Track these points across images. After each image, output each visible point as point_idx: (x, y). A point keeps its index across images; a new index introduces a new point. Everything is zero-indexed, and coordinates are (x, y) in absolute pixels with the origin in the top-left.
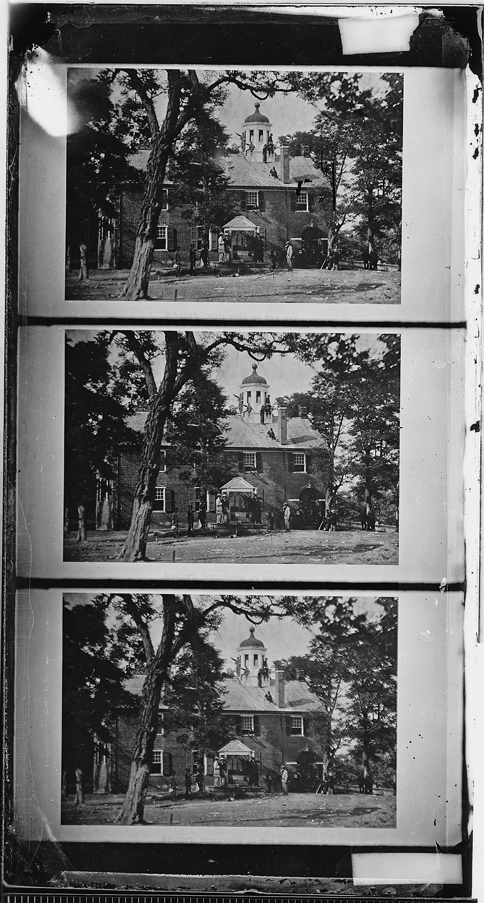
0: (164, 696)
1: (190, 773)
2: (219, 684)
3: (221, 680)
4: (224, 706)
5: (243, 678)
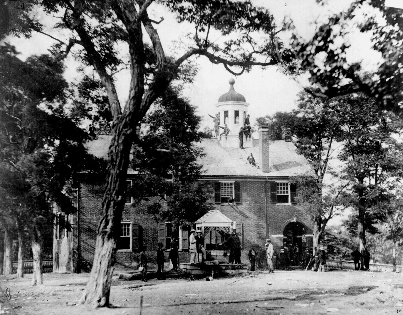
1: (163, 248)
2: (196, 145)
4: (201, 170)
5: (222, 138)
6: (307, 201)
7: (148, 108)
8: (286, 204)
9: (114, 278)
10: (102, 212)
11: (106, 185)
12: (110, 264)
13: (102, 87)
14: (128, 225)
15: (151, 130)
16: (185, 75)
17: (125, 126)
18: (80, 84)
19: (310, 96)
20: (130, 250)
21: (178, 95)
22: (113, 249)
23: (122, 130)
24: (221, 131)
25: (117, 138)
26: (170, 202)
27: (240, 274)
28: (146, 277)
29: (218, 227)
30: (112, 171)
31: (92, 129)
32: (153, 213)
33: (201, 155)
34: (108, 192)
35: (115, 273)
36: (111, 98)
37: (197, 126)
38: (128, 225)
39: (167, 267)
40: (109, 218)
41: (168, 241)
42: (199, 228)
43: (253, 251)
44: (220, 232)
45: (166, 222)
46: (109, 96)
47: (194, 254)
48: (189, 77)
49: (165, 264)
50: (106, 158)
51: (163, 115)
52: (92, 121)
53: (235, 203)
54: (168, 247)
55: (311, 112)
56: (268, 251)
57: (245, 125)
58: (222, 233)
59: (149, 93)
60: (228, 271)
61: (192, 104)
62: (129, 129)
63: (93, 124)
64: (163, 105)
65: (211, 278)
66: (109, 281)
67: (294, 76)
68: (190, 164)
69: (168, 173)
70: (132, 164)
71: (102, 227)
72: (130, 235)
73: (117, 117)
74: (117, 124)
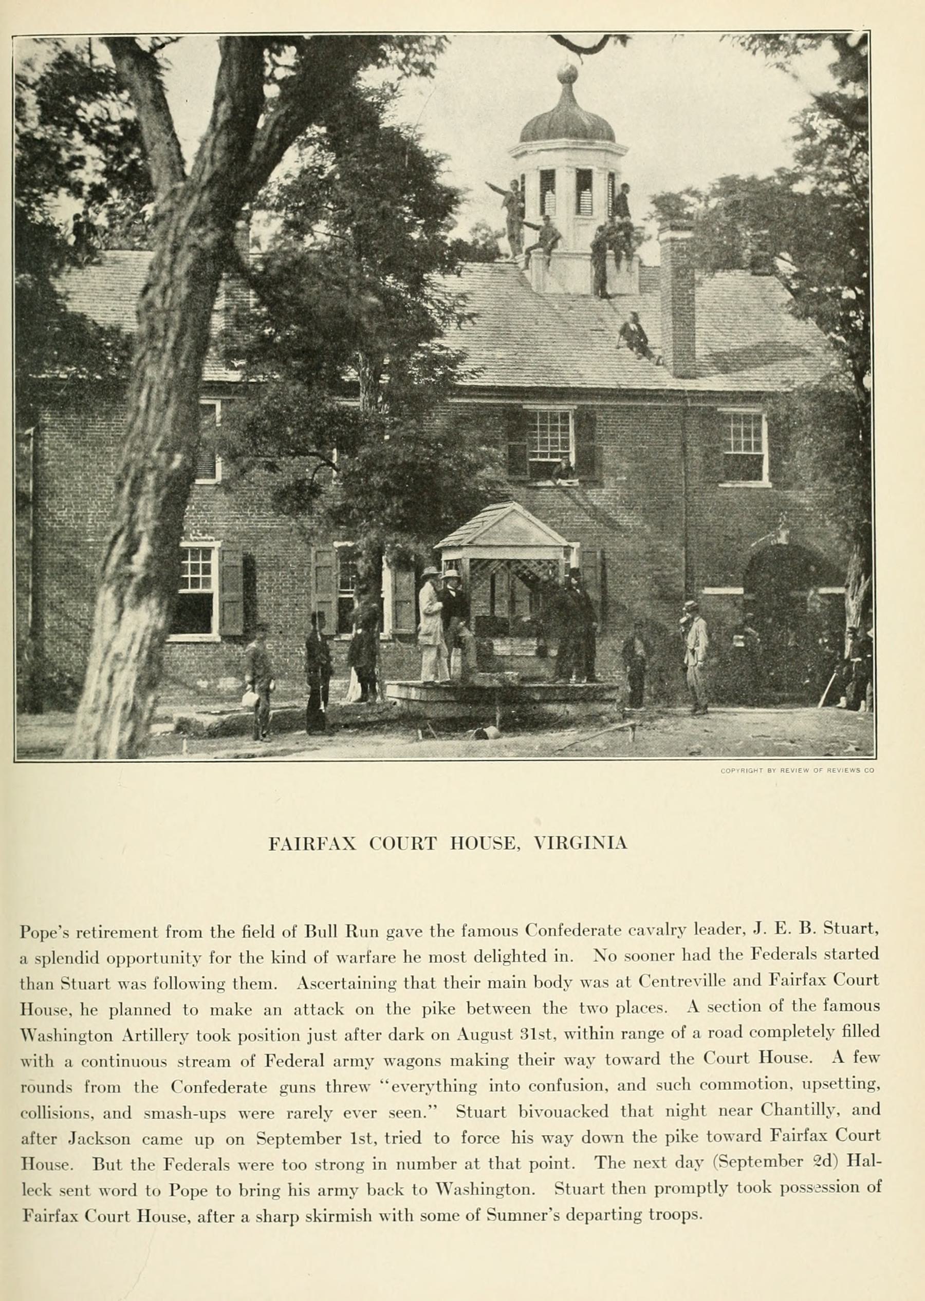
0: (225, 334)
1: (326, 631)
2: (443, 284)
3: (449, 267)
4: (461, 368)
5: (533, 263)
6: (826, 474)
7: (277, 158)
8: (753, 484)
9: (157, 729)
10: (115, 511)
11: (130, 416)
12: (144, 682)
13: (119, 90)
14: (207, 552)
15: (286, 232)
16: (407, 52)
17: (197, 220)
18: (42, 79)
19: (835, 123)
20: (214, 635)
21: (382, 116)
22: (155, 634)
23: (186, 234)
24: (530, 237)
25: (167, 259)
26: (353, 473)
27: (594, 720)
28: (266, 726)
29: (519, 561)
30: (149, 372)
31: (84, 228)
32: (292, 512)
33: (461, 318)
34: (138, 442)
35: (160, 711)
36: (150, 129)
37: (446, 221)
38: (207, 552)
39: (341, 695)
40: (140, 527)
41: (344, 606)
42: (452, 564)
43: (638, 642)
44: (524, 578)
45: (337, 544)
46: (143, 119)
47: (434, 653)
48: (420, 58)
49: (335, 684)
50: (131, 326)
51: (330, 181)
52: (82, 201)
53: (576, 482)
54: (344, 626)
55: (842, 178)
56: (690, 641)
57: (612, 219)
58: (532, 582)
59: (282, 112)
60: (551, 708)
61: (428, 146)
62: (212, 230)
63: (86, 213)
64: (330, 149)
65: (491, 730)
66: (139, 740)
67: (780, 56)
68: (421, 350)
69: (346, 379)
70: (222, 347)
71: (114, 560)
72: (214, 588)
73: (168, 188)
74: (171, 211)
